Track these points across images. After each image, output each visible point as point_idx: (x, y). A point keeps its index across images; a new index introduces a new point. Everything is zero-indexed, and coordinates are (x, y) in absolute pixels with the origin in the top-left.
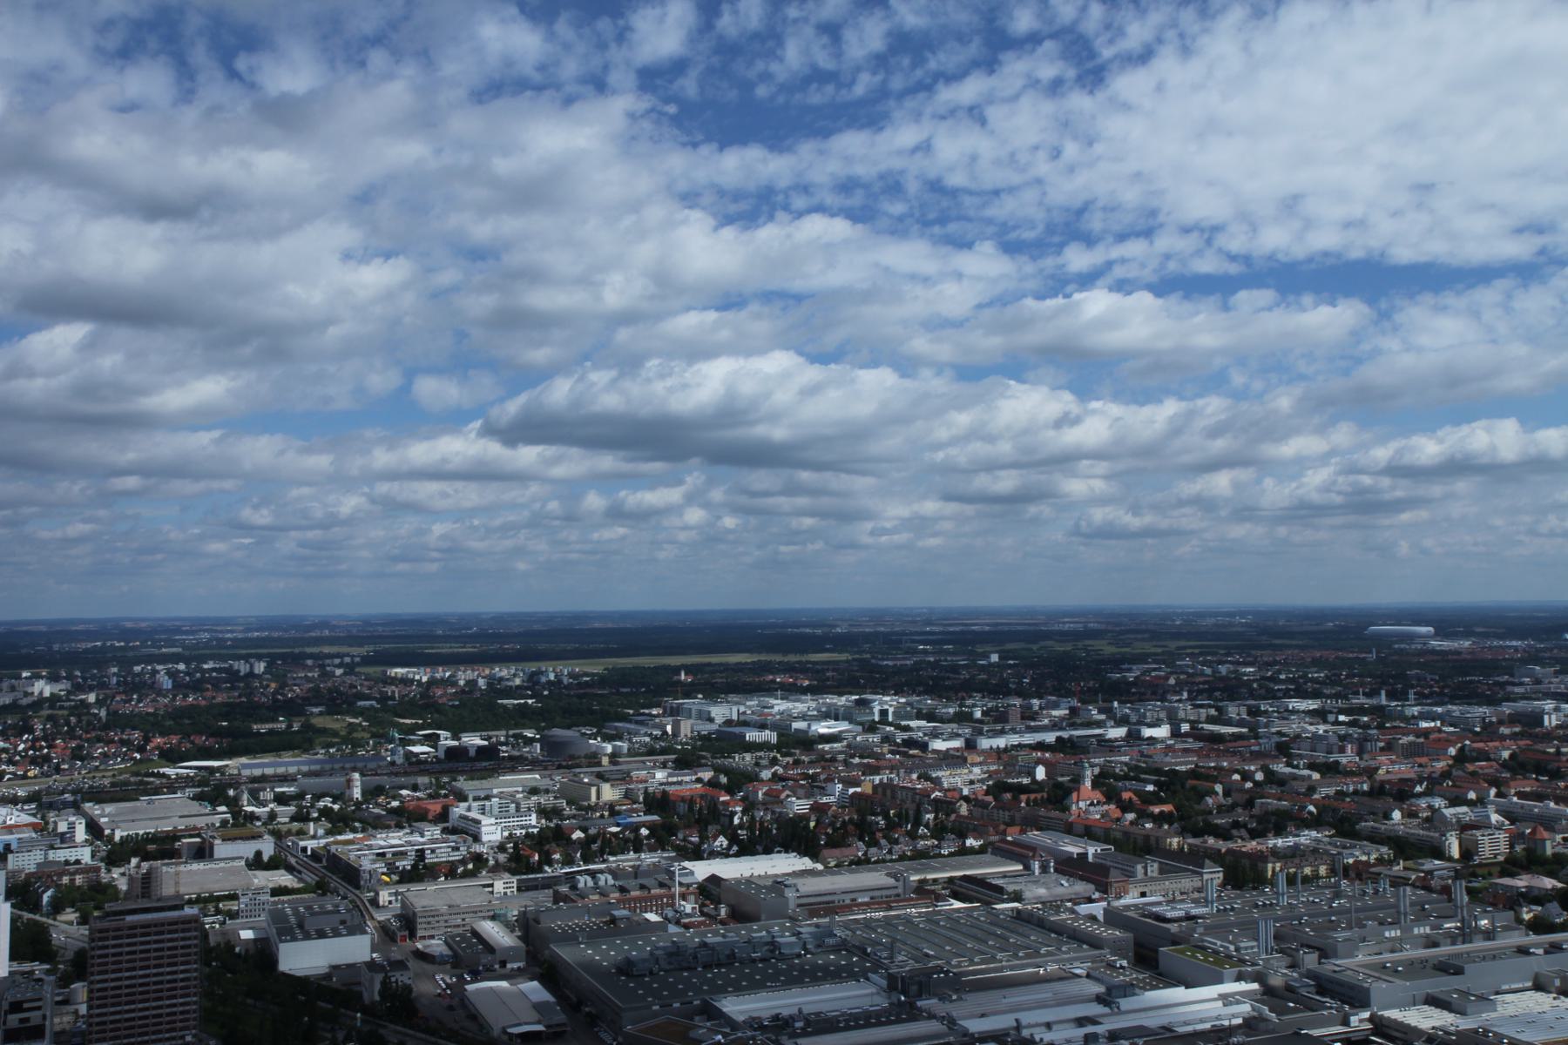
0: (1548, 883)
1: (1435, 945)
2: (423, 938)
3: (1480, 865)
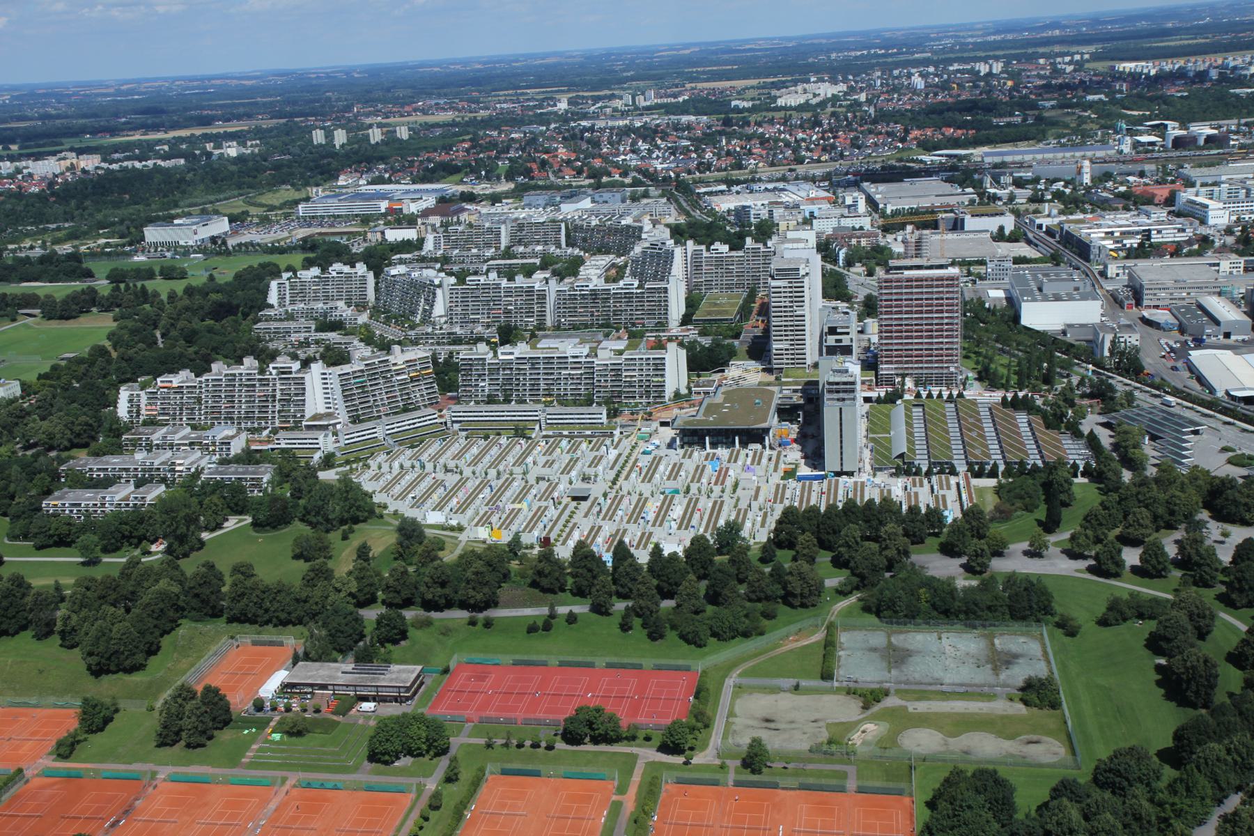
2: (1149, 307)
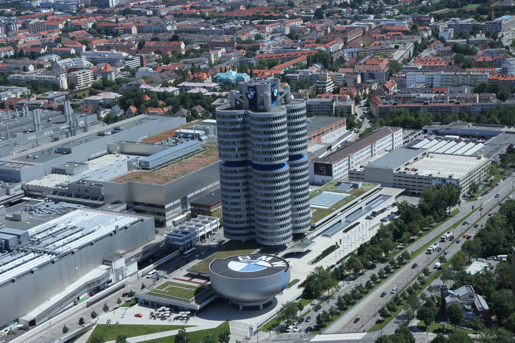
0: (113, 95)
1: (56, 139)
3: (79, 91)
